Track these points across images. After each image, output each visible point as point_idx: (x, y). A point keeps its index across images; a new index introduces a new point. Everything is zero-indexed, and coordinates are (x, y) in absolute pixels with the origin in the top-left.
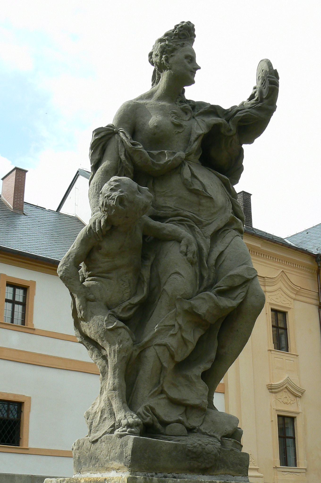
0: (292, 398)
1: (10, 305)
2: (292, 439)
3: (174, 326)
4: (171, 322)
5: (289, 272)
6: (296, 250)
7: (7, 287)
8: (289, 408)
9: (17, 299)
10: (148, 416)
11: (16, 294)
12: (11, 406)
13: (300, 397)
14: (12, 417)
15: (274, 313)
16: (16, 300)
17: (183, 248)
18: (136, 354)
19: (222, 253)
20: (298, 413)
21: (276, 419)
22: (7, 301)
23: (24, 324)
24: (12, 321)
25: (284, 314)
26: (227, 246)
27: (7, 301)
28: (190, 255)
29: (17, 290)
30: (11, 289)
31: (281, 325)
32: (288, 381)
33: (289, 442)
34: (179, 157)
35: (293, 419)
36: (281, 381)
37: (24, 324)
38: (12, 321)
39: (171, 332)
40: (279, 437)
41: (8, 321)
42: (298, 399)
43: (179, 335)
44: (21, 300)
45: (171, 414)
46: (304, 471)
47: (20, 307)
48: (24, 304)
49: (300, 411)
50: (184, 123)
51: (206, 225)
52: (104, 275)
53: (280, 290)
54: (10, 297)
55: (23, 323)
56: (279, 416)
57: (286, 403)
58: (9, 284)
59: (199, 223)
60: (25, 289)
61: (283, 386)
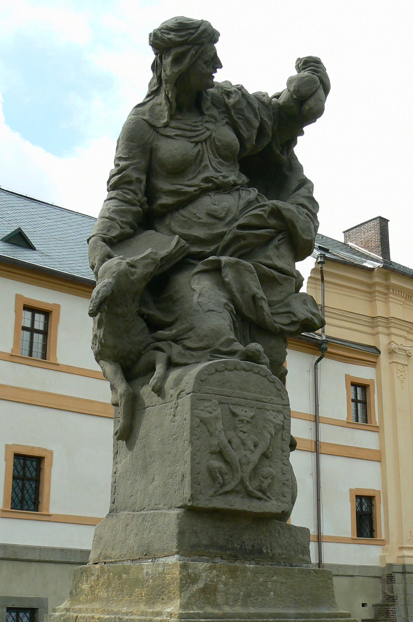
1: (27, 334)
7: (24, 312)
9: (36, 327)
24: (31, 354)
27: (24, 328)
29: (37, 316)
30: (28, 314)
41: (26, 354)
44: (41, 328)
47: (41, 336)
48: (45, 333)
54: (28, 324)
55: (44, 356)
58: (26, 308)
60: (47, 314)
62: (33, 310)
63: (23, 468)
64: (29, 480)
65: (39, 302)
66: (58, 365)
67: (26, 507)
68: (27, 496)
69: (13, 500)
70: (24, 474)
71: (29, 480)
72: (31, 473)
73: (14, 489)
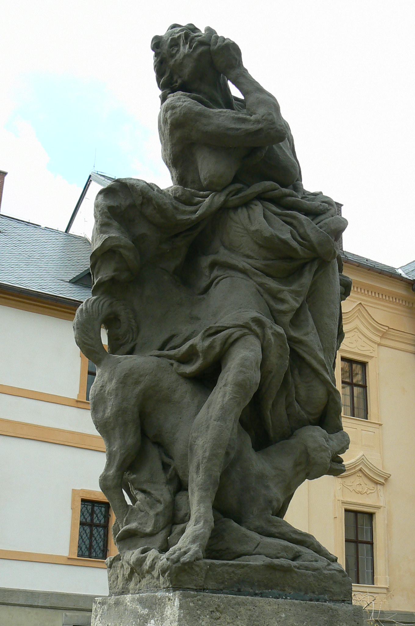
0: (371, 485)
2: (369, 546)
5: (371, 305)
6: (380, 273)
8: (363, 500)
12: (96, 508)
13: (382, 484)
14: (98, 522)
15: (346, 364)
20: (379, 508)
21: (342, 515)
25: (364, 365)
31: (357, 379)
32: (362, 460)
33: (364, 548)
35: (371, 515)
36: (353, 460)
40: (346, 541)
42: (379, 487)
46: (385, 591)
49: (381, 504)
53: (356, 330)
56: (346, 511)
57: (360, 493)
61: (355, 468)
63: (92, 515)
64: (97, 526)
67: (94, 554)
68: (94, 543)
69: (80, 547)
70: (92, 520)
71: (97, 526)
72: (99, 519)
73: (81, 536)
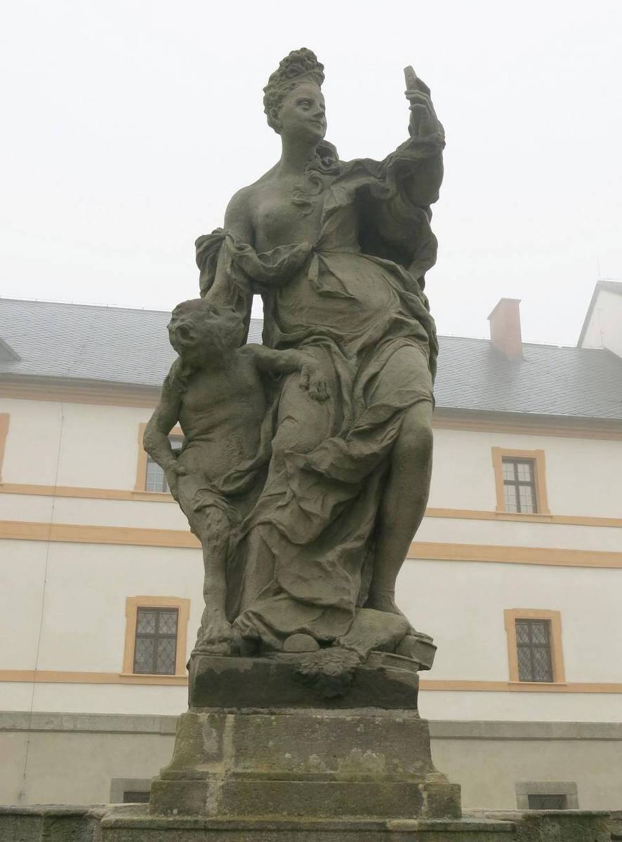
1: (512, 489)
3: (285, 493)
4: (280, 490)
7: (504, 465)
9: (520, 479)
10: (248, 626)
11: (519, 471)
16: (520, 479)
17: (303, 380)
18: (235, 541)
19: (374, 377)
22: (507, 483)
23: (538, 511)
24: (519, 509)
26: (385, 365)
27: (507, 483)
28: (313, 389)
30: (510, 467)
34: (300, 250)
37: (538, 511)
38: (519, 509)
39: (280, 503)
43: (293, 506)
44: (528, 479)
45: (284, 617)
47: (529, 489)
48: (532, 484)
50: (312, 200)
51: (351, 340)
52: (198, 437)
54: (512, 478)
55: (535, 509)
58: (506, 460)
59: (338, 340)
60: (531, 462)
62: (515, 460)
65: (518, 451)
66: (551, 517)
